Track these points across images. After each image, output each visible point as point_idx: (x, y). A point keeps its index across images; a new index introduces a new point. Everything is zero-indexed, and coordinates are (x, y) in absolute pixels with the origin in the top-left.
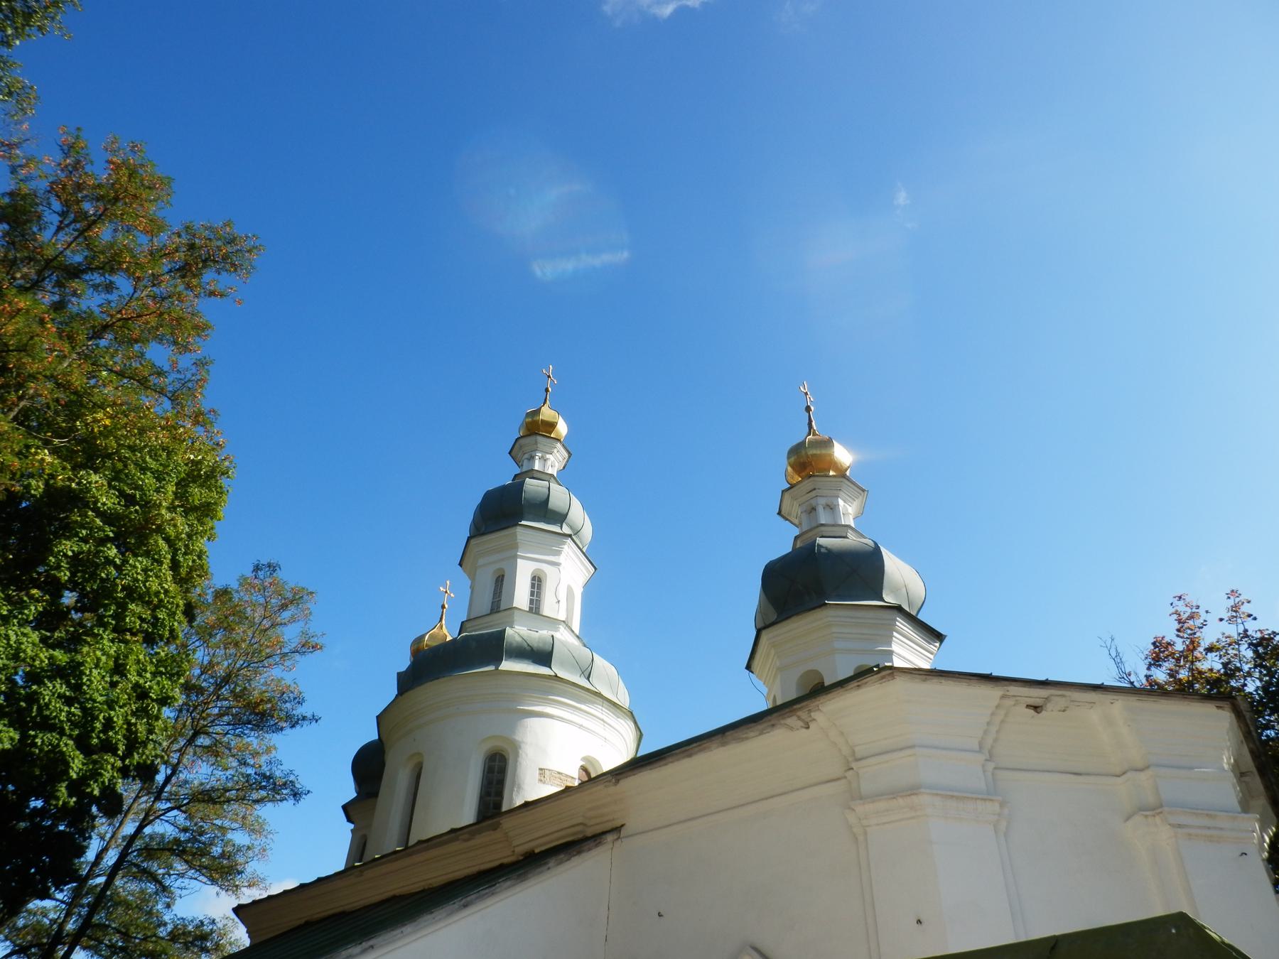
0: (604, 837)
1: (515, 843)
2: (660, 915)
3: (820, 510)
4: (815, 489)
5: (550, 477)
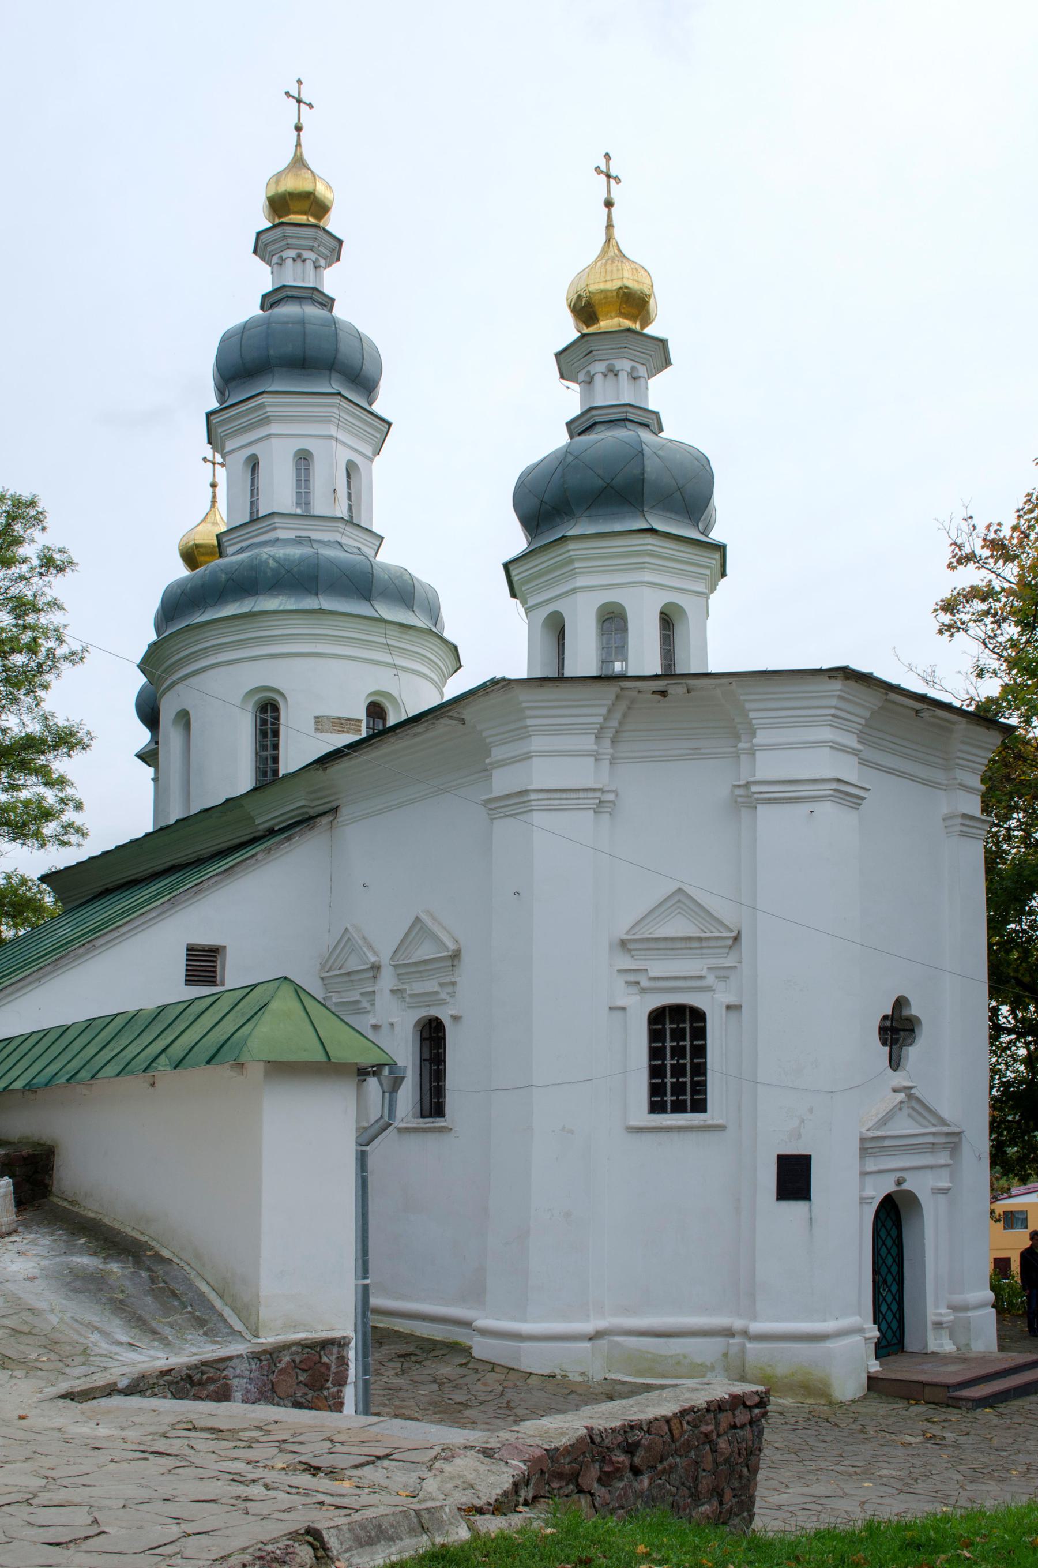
0: (318, 820)
1: (257, 822)
2: (365, 885)
3: (599, 379)
4: (591, 351)
5: (311, 291)
